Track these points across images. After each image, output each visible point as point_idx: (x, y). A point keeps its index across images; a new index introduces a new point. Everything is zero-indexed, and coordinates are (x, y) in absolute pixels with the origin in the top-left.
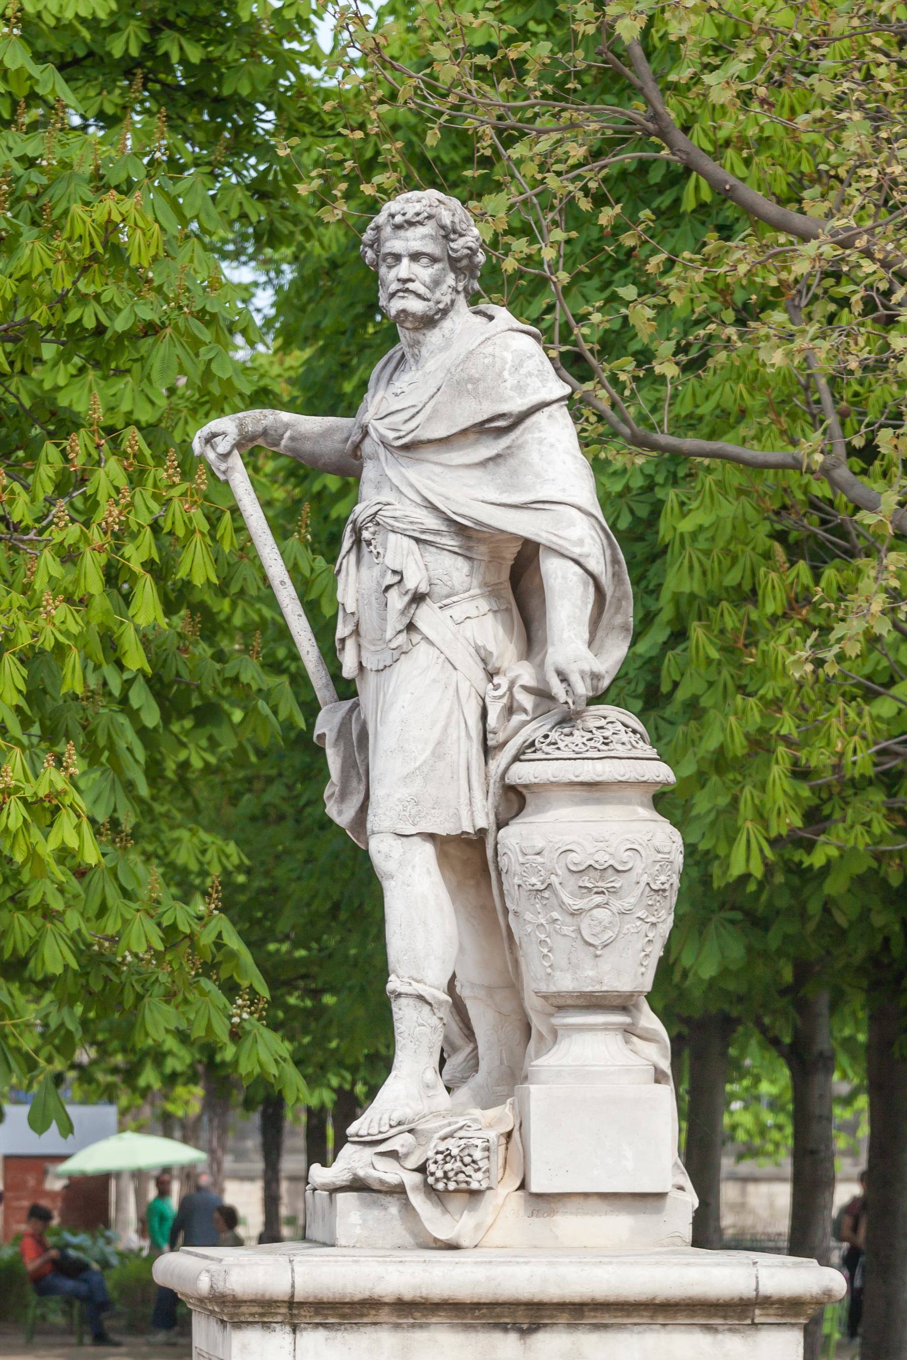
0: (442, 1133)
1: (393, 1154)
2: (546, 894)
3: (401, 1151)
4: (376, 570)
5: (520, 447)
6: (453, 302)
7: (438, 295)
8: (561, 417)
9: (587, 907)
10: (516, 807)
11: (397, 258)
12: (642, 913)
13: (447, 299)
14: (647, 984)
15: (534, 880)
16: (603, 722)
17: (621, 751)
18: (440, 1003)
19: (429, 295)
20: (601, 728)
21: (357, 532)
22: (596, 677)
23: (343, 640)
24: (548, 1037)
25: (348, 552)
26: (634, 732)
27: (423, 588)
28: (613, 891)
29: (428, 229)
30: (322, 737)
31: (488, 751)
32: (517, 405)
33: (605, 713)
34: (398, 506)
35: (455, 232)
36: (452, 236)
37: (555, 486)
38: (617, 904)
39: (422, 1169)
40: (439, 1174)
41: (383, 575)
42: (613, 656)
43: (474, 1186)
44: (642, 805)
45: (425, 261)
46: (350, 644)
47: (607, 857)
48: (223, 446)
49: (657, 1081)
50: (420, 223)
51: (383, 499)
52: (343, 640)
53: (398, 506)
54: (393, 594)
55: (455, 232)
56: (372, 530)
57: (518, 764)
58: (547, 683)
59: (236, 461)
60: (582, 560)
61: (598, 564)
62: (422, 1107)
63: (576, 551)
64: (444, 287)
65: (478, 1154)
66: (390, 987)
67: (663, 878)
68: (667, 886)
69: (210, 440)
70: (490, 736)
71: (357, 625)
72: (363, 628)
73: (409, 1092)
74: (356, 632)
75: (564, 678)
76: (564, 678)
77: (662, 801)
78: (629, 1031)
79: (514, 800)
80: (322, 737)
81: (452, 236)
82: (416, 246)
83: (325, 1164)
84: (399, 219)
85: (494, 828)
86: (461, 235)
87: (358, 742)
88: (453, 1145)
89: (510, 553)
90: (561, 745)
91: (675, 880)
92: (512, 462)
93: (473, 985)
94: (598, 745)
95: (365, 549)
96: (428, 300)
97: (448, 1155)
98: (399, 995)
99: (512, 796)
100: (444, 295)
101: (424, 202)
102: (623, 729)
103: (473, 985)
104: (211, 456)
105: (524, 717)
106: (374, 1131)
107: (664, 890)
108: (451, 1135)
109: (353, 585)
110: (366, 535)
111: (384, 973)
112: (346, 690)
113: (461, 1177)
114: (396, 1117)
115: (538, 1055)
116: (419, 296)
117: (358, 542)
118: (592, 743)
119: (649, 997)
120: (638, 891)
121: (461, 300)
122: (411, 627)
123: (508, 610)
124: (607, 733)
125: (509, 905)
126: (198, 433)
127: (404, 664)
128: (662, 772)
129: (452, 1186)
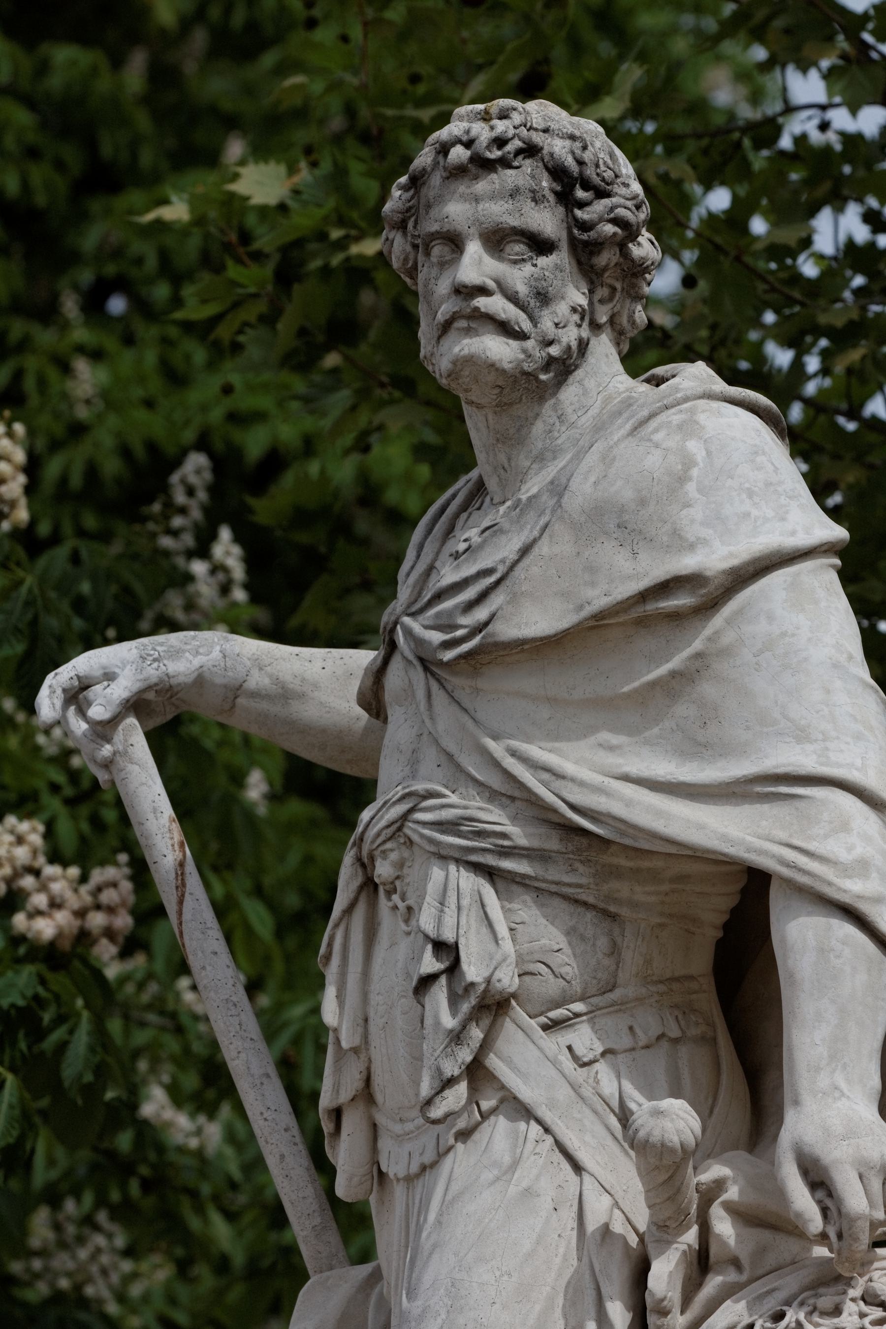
4: (403, 948)
5: (726, 652)
6: (583, 346)
7: (547, 324)
8: (823, 584)
11: (455, 242)
13: (570, 336)
19: (526, 325)
21: (365, 865)
25: (349, 910)
27: (507, 979)
29: (525, 174)
32: (715, 557)
34: (453, 799)
35: (586, 185)
36: (580, 194)
41: (417, 958)
45: (519, 248)
46: (352, 1123)
48: (103, 703)
50: (505, 163)
51: (420, 787)
52: (337, 1114)
53: (453, 799)
54: (440, 993)
55: (586, 185)
56: (394, 856)
58: (781, 1194)
59: (134, 740)
60: (865, 908)
63: (852, 888)
64: (562, 309)
69: (77, 696)
71: (368, 1081)
72: (378, 1081)
74: (367, 1094)
75: (819, 1181)
76: (819, 1181)
81: (580, 194)
82: (499, 212)
86: (602, 194)
89: (714, 908)
92: (707, 689)
95: (384, 904)
96: (521, 336)
101: (517, 118)
104: (79, 726)
105: (732, 1276)
110: (383, 870)
116: (505, 329)
117: (369, 886)
121: (604, 353)
122: (477, 1072)
126: (49, 679)
127: (462, 1161)
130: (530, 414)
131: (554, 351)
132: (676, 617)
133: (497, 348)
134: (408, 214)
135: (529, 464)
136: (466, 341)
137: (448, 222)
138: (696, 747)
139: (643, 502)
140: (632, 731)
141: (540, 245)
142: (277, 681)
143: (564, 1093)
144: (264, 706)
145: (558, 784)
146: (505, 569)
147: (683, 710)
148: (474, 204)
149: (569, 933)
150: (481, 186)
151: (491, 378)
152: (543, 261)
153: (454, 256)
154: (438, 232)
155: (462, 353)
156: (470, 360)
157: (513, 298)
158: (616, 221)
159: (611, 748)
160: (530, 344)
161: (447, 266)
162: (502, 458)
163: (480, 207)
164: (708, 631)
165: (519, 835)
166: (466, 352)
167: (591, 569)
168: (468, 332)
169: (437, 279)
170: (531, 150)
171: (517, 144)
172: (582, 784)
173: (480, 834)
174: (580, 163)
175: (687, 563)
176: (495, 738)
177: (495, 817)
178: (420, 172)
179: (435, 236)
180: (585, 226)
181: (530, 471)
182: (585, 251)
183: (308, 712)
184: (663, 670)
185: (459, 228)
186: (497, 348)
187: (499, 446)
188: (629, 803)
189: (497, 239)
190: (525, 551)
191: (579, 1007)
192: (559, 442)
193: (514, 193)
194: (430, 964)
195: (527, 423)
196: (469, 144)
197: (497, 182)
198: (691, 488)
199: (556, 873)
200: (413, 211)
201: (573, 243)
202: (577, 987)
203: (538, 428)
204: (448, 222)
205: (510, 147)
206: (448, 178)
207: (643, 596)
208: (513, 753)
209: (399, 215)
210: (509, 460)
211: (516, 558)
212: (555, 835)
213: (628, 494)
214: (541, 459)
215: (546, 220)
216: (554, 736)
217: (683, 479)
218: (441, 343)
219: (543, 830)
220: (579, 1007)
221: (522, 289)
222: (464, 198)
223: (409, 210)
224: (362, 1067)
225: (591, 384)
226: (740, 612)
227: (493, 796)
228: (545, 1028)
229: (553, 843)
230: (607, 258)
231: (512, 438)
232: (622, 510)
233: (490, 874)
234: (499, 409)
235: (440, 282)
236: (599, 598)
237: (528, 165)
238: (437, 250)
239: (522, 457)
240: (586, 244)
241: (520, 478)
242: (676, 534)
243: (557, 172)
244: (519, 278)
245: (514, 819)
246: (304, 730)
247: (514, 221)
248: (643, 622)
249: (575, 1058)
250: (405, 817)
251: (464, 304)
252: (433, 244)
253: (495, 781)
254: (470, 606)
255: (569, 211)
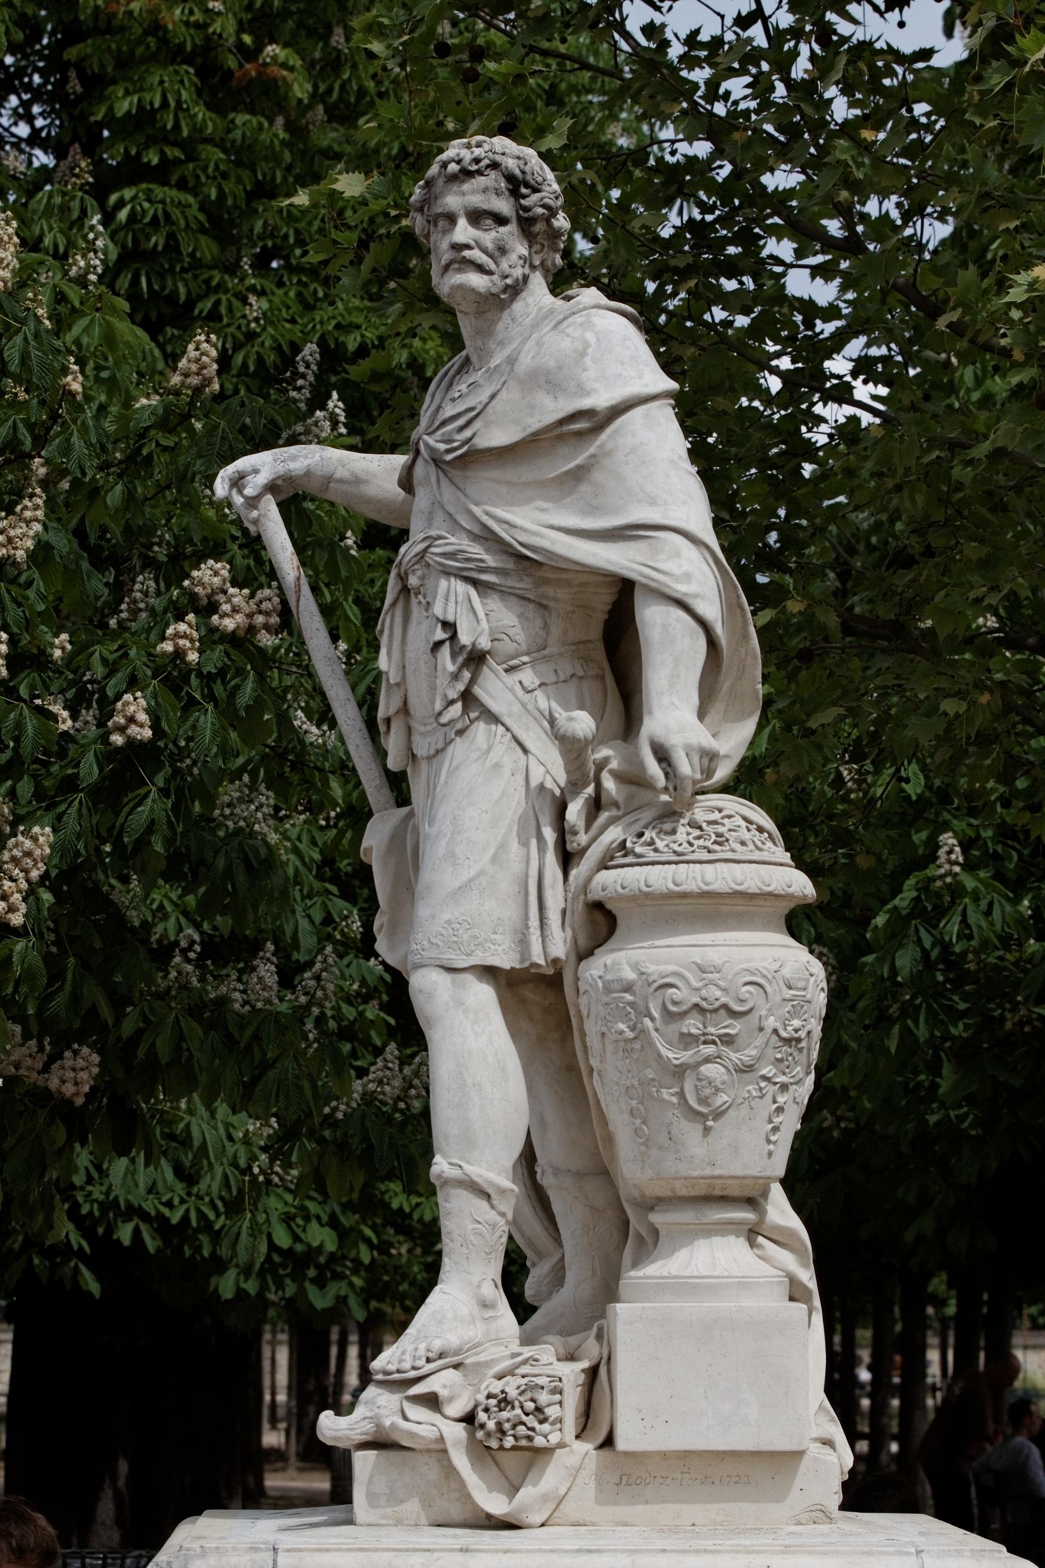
0: (498, 1368)
1: (432, 1401)
2: (637, 1045)
3: (443, 1393)
4: (425, 625)
5: (608, 454)
6: (526, 278)
7: (504, 265)
9: (691, 1061)
10: (604, 930)
11: (451, 219)
12: (768, 1070)
13: (518, 272)
14: (781, 1171)
15: (622, 1026)
16: (716, 816)
17: (741, 853)
18: (503, 1192)
19: (492, 266)
20: (715, 822)
21: (403, 578)
22: (710, 758)
23: (388, 721)
24: (649, 1240)
25: (394, 604)
26: (761, 829)
27: (484, 643)
28: (728, 1040)
30: (369, 850)
31: (567, 859)
32: (601, 399)
33: (720, 804)
34: (453, 540)
35: (527, 185)
36: (524, 190)
37: (655, 505)
38: (735, 1056)
39: (469, 1419)
40: (491, 1425)
42: (735, 739)
43: (539, 1441)
44: (777, 930)
45: (489, 222)
47: (718, 993)
49: (792, 1299)
50: (480, 173)
51: (433, 533)
52: (388, 721)
53: (453, 540)
55: (527, 185)
57: (604, 873)
58: (641, 765)
59: (270, 509)
60: (690, 601)
61: (711, 610)
62: (474, 1332)
63: (681, 589)
64: (513, 257)
65: (543, 1398)
66: (435, 1170)
67: (796, 1023)
68: (802, 1034)
70: (568, 837)
71: (405, 702)
72: (413, 701)
73: (460, 1312)
74: (405, 709)
75: (663, 755)
76: (663, 755)
77: (799, 922)
78: (752, 1234)
79: (601, 923)
80: (369, 850)
81: (524, 190)
82: (477, 200)
83: (338, 1414)
84: (453, 167)
85: (573, 959)
86: (536, 190)
87: (408, 854)
88: (511, 1387)
89: (603, 601)
90: (660, 844)
91: (816, 1027)
92: (597, 475)
93: (557, 1171)
94: (708, 844)
95: (414, 600)
96: (490, 273)
97: (504, 1402)
98: (446, 1182)
99: (599, 917)
100: (513, 264)
101: (486, 147)
102: (744, 824)
103: (557, 1171)
104: (238, 500)
105: (614, 812)
106: (407, 1365)
107: (799, 1040)
108: (511, 1372)
109: (402, 652)
110: (413, 581)
111: (428, 1152)
112: (399, 787)
113: (522, 1430)
114: (437, 1345)
115: (636, 1264)
116: (481, 269)
117: (405, 591)
118: (701, 842)
119: (783, 1182)
120: (760, 1040)
121: (538, 284)
122: (468, 698)
123: (602, 678)
124: (721, 829)
125: (592, 1062)
126: (222, 473)
127: (459, 748)
128: (800, 885)
129: (509, 1442)
131: (509, 281)
132: (580, 434)
133: (476, 280)
138: (593, 509)
139: (560, 368)
140: (555, 500)
141: (501, 220)
142: (353, 474)
143: (517, 708)
144: (346, 487)
145: (513, 531)
147: (584, 488)
149: (520, 616)
150: (466, 187)
151: (473, 297)
152: (502, 229)
156: (461, 287)
157: (485, 251)
158: (544, 206)
159: (543, 510)
160: (495, 277)
162: (480, 343)
164: (598, 442)
165: (490, 560)
167: (531, 407)
168: (459, 270)
170: (494, 165)
171: (487, 161)
172: (526, 530)
173: (468, 560)
174: (523, 172)
175: (586, 403)
176: (477, 504)
177: (476, 550)
179: (439, 215)
180: (526, 209)
182: (526, 224)
183: (371, 490)
184: (572, 465)
186: (476, 280)
188: (553, 542)
189: (476, 217)
190: (493, 397)
191: (525, 659)
193: (485, 190)
194: (440, 634)
195: (494, 323)
196: (459, 162)
198: (588, 360)
199: (510, 582)
201: (520, 219)
202: (524, 647)
203: (500, 326)
205: (483, 164)
207: (561, 422)
208: (487, 513)
212: (511, 560)
213: (552, 364)
214: (501, 343)
215: (504, 206)
216: (510, 503)
217: (583, 354)
219: (504, 557)
220: (525, 659)
221: (490, 246)
224: (401, 693)
225: (530, 300)
226: (616, 431)
227: (475, 537)
228: (506, 671)
229: (510, 564)
230: (539, 227)
231: (486, 332)
232: (549, 372)
233: (475, 583)
236: (536, 423)
237: (493, 174)
238: (441, 223)
240: (527, 219)
242: (580, 386)
243: (510, 178)
244: (489, 238)
245: (488, 551)
246: (368, 501)
247: (485, 206)
248: (560, 437)
249: (523, 688)
250: (425, 550)
253: (476, 530)
254: (461, 429)
255: (517, 200)
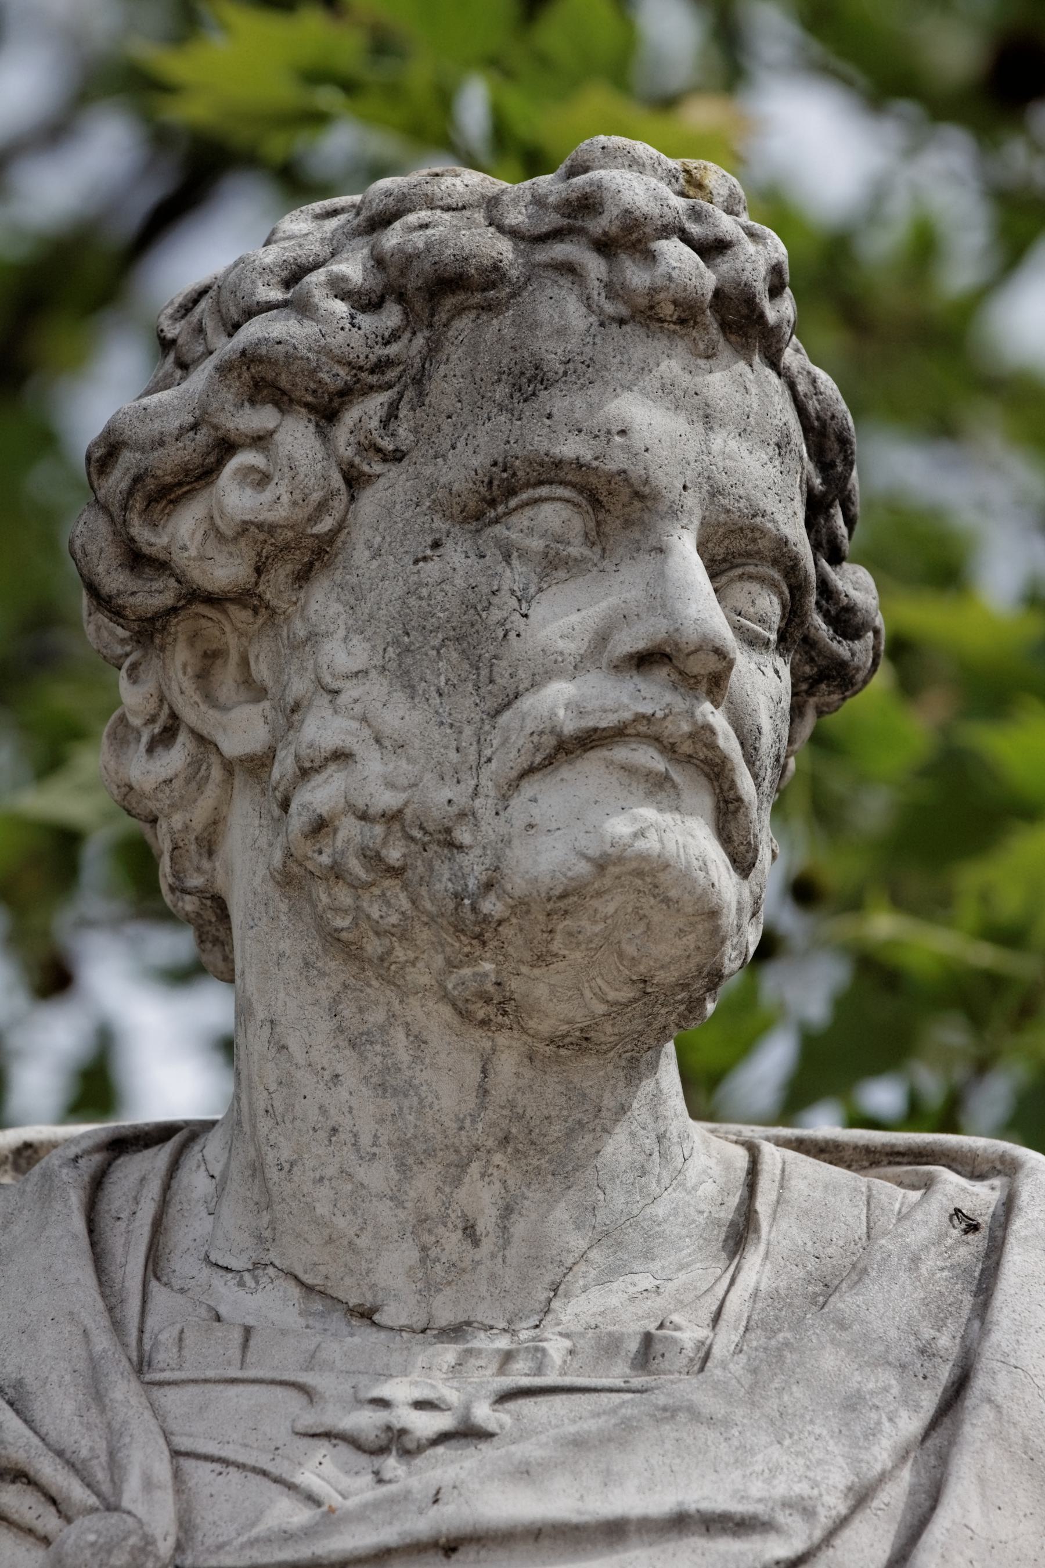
130: (609, 1101)
134: (373, 379)
135: (583, 1244)
136: (648, 813)
137: (622, 447)
146: (818, 1534)
148: (699, 427)
153: (587, 552)
154: (579, 465)
155: (641, 845)
161: (561, 574)
162: (481, 1197)
163: (718, 441)
166: (650, 844)
168: (658, 786)
169: (523, 598)
178: (481, 270)
179: (552, 471)
181: (582, 1267)
185: (660, 478)
187: (498, 1158)
192: (660, 1210)
197: (754, 390)
200: (391, 374)
204: (627, 449)
206: (622, 322)
209: (342, 372)
210: (507, 1211)
211: (843, 1510)
218: (524, 784)
222: (669, 394)
223: (381, 366)
234: (550, 1050)
235: (537, 612)
238: (554, 516)
239: (561, 1213)
241: (548, 1278)
251: (678, 702)
252: (544, 491)
